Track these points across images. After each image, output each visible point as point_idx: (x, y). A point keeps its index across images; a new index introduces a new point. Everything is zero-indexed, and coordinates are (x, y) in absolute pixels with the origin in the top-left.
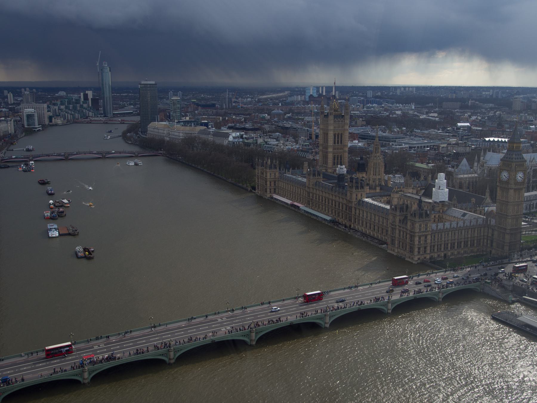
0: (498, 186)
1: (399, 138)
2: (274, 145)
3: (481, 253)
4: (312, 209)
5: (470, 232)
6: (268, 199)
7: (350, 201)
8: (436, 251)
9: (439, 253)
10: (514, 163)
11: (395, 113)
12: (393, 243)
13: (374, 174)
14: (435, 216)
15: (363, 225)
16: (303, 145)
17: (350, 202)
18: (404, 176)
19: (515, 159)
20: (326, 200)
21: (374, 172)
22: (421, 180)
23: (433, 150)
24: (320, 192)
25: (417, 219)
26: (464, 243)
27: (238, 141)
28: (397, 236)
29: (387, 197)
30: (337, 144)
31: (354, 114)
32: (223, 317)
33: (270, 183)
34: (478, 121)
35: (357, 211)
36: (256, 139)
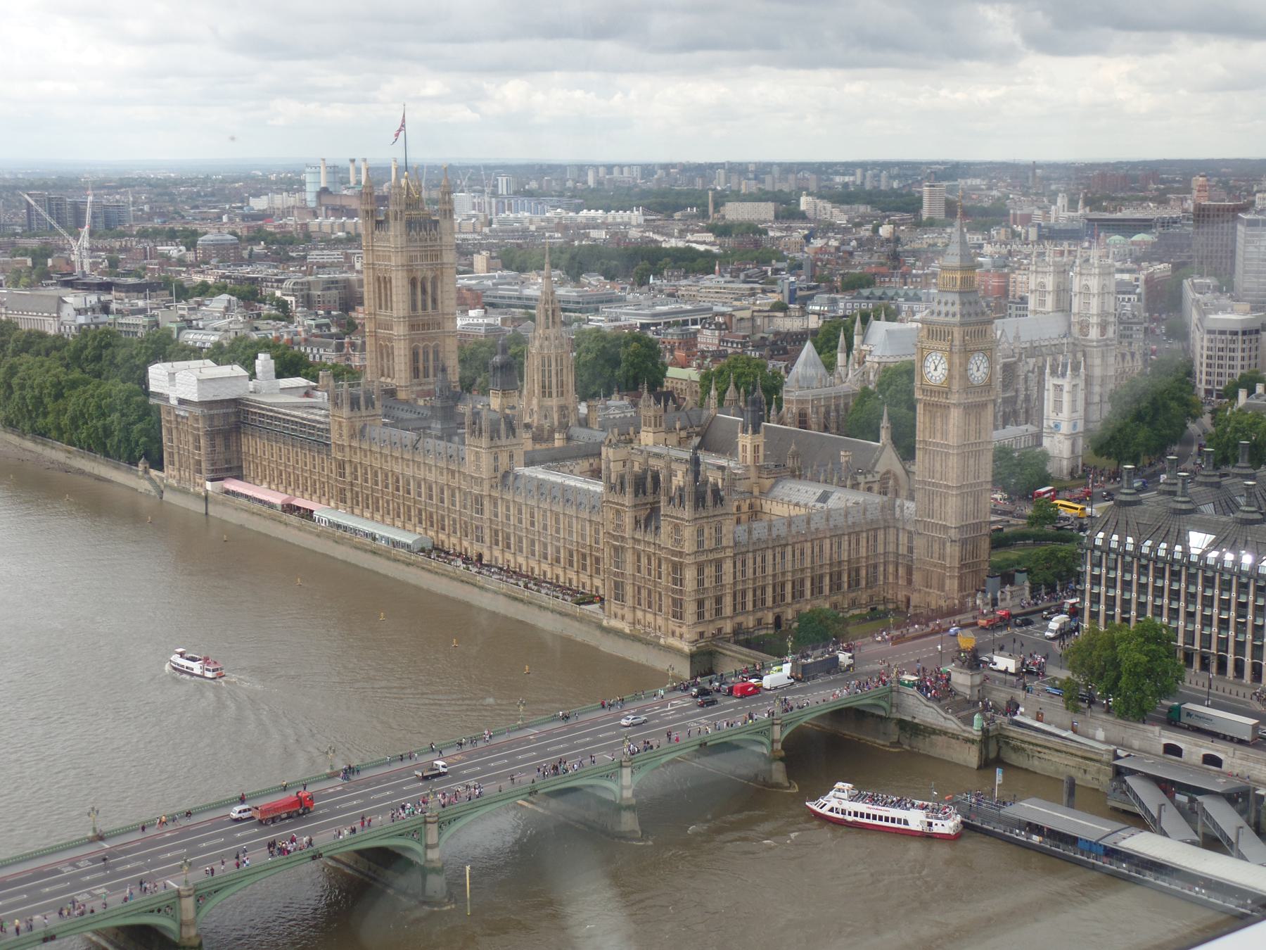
0: (917, 400)
1: (610, 301)
2: (216, 329)
3: (881, 607)
4: (353, 513)
5: (845, 545)
7: (476, 478)
8: (751, 609)
9: (759, 615)
11: (587, 236)
12: (620, 597)
13: (544, 396)
14: (739, 508)
15: (521, 551)
16: (310, 326)
17: (479, 481)
18: (635, 405)
19: (962, 315)
22: (689, 407)
23: (713, 327)
25: (687, 513)
26: (831, 580)
28: (629, 569)
29: (591, 461)
30: (420, 312)
31: (464, 240)
32: (78, 859)
34: (833, 250)
35: (501, 509)
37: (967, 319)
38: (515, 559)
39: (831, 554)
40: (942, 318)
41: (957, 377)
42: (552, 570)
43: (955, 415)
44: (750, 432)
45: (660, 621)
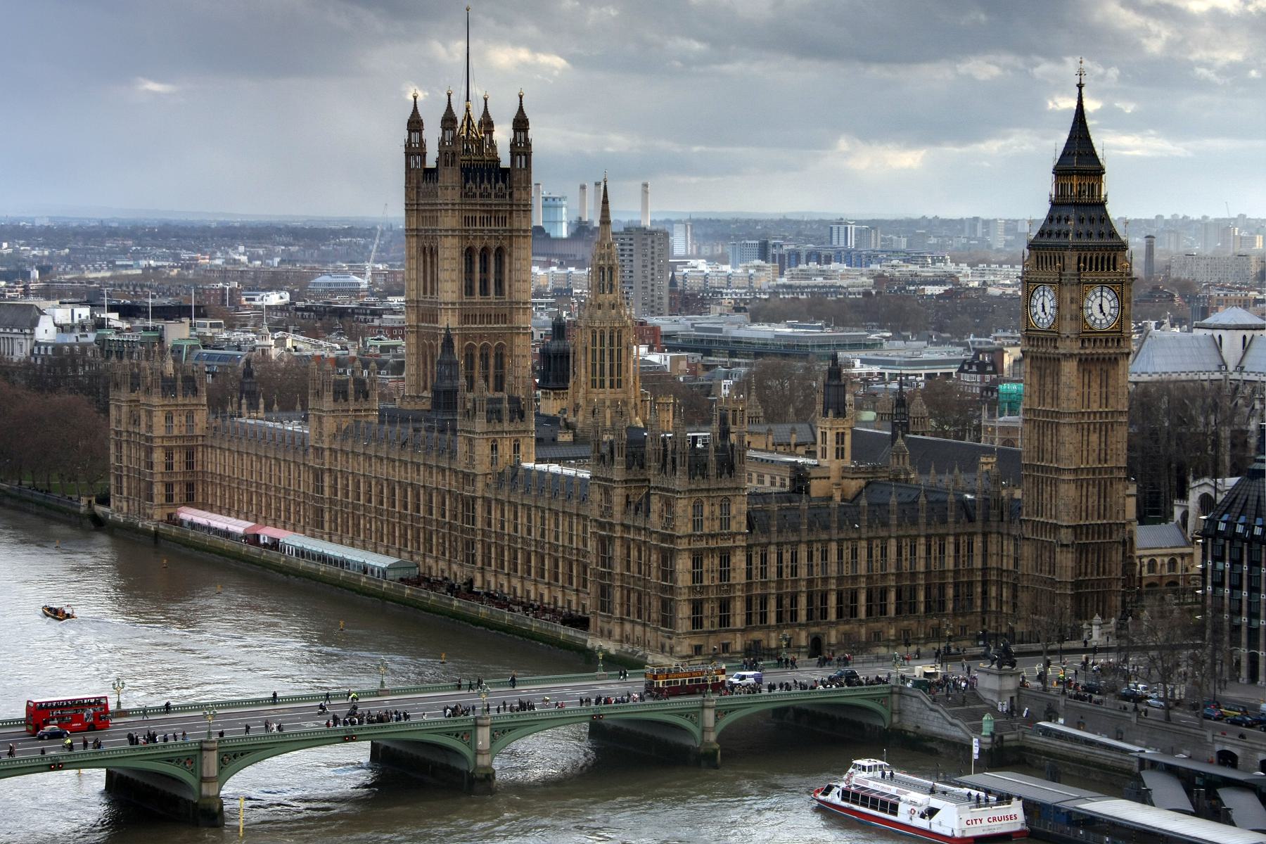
4: (331, 541)
5: (921, 550)
6: (156, 535)
7: (466, 476)
10: (1076, 254)
12: (604, 604)
13: (594, 386)
15: (516, 571)
19: (1079, 235)
20: (382, 492)
21: (594, 373)
23: (974, 369)
24: (359, 464)
25: (679, 481)
26: (899, 597)
27: (82, 340)
30: (477, 297)
33: (169, 453)
35: (495, 515)
36: (160, 323)
37: (1084, 241)
38: (509, 582)
39: (899, 561)
40: (1053, 240)
41: (1068, 316)
42: (550, 592)
43: (1069, 369)
44: (831, 413)
45: (650, 635)
